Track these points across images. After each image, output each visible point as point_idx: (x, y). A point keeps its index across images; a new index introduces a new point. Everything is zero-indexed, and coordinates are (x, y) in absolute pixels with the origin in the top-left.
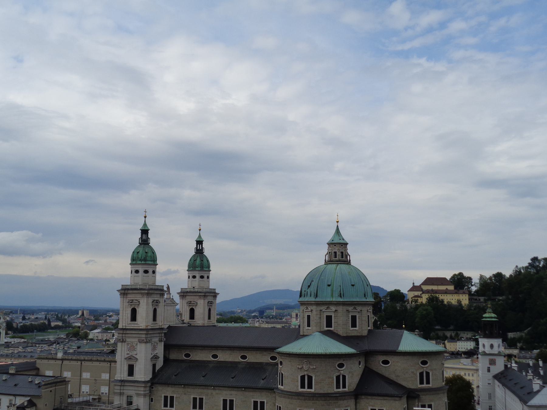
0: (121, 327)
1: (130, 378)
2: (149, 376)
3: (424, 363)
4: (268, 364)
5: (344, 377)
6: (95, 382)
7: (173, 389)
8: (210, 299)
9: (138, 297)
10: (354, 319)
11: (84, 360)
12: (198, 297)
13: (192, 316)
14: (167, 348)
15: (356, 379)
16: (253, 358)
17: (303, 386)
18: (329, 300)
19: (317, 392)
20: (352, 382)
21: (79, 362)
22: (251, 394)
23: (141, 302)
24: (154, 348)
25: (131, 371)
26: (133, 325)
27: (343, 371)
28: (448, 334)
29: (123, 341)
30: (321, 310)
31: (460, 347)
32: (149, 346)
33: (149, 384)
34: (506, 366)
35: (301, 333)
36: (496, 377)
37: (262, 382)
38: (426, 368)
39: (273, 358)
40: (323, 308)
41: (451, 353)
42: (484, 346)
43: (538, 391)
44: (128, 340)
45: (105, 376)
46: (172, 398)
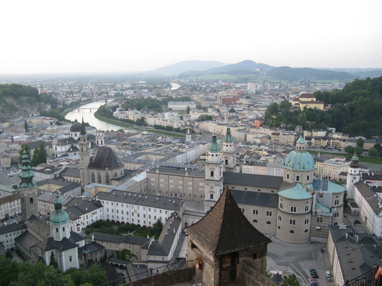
0: (207, 179)
1: (212, 200)
3: (337, 197)
4: (270, 194)
5: (308, 207)
9: (214, 167)
10: (308, 177)
11: (170, 175)
12: (229, 155)
18: (298, 170)
19: (298, 213)
21: (167, 176)
23: (216, 169)
24: (220, 187)
25: (212, 196)
26: (212, 178)
29: (208, 185)
30: (295, 174)
31: (320, 134)
36: (355, 184)
37: (270, 203)
40: (296, 173)
41: (316, 138)
42: (351, 171)
44: (210, 184)
45: (181, 182)
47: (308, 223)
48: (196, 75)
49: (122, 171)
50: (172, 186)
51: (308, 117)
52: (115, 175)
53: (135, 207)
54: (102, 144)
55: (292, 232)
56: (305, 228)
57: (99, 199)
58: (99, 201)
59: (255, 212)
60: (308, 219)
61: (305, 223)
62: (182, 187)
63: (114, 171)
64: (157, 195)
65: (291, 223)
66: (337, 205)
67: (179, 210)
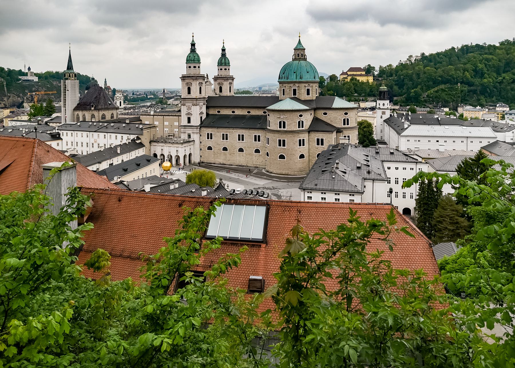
1: (189, 124)
2: (198, 123)
3: (346, 114)
4: (262, 116)
5: (303, 122)
6: (171, 126)
7: (212, 130)
8: (230, 81)
10: (308, 90)
11: (165, 115)
13: (221, 91)
14: (207, 108)
15: (309, 123)
16: (254, 112)
17: (280, 127)
20: (307, 125)
22: (253, 131)
24: (201, 108)
27: (302, 119)
28: (361, 98)
32: (198, 107)
33: (199, 127)
34: (391, 115)
35: (280, 99)
36: (385, 121)
37: (259, 125)
38: (347, 117)
39: (265, 112)
40: (292, 85)
43: (407, 128)
45: (176, 124)
46: (211, 134)
47: (304, 145)
48: (269, 86)
49: (112, 114)
50: (167, 129)
51: (354, 89)
52: (104, 117)
53: (96, 134)
54: (120, 106)
55: (282, 157)
56: (300, 152)
57: (58, 131)
58: (59, 132)
59: (241, 138)
60: (303, 140)
61: (300, 145)
62: (178, 130)
63: (101, 113)
64: (127, 122)
65: (280, 145)
66: (346, 126)
67: (142, 134)
